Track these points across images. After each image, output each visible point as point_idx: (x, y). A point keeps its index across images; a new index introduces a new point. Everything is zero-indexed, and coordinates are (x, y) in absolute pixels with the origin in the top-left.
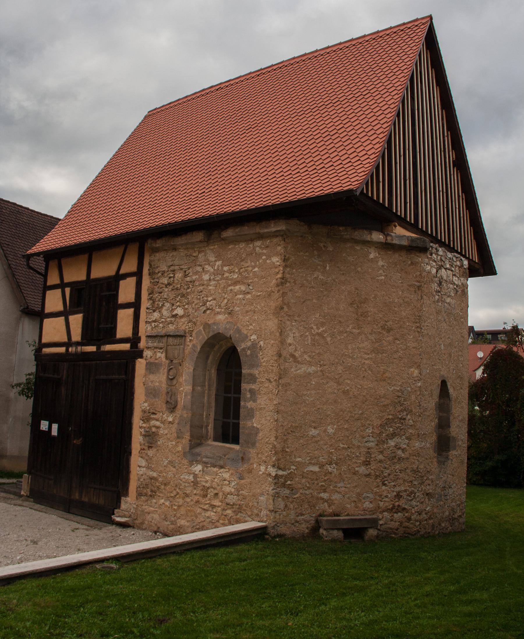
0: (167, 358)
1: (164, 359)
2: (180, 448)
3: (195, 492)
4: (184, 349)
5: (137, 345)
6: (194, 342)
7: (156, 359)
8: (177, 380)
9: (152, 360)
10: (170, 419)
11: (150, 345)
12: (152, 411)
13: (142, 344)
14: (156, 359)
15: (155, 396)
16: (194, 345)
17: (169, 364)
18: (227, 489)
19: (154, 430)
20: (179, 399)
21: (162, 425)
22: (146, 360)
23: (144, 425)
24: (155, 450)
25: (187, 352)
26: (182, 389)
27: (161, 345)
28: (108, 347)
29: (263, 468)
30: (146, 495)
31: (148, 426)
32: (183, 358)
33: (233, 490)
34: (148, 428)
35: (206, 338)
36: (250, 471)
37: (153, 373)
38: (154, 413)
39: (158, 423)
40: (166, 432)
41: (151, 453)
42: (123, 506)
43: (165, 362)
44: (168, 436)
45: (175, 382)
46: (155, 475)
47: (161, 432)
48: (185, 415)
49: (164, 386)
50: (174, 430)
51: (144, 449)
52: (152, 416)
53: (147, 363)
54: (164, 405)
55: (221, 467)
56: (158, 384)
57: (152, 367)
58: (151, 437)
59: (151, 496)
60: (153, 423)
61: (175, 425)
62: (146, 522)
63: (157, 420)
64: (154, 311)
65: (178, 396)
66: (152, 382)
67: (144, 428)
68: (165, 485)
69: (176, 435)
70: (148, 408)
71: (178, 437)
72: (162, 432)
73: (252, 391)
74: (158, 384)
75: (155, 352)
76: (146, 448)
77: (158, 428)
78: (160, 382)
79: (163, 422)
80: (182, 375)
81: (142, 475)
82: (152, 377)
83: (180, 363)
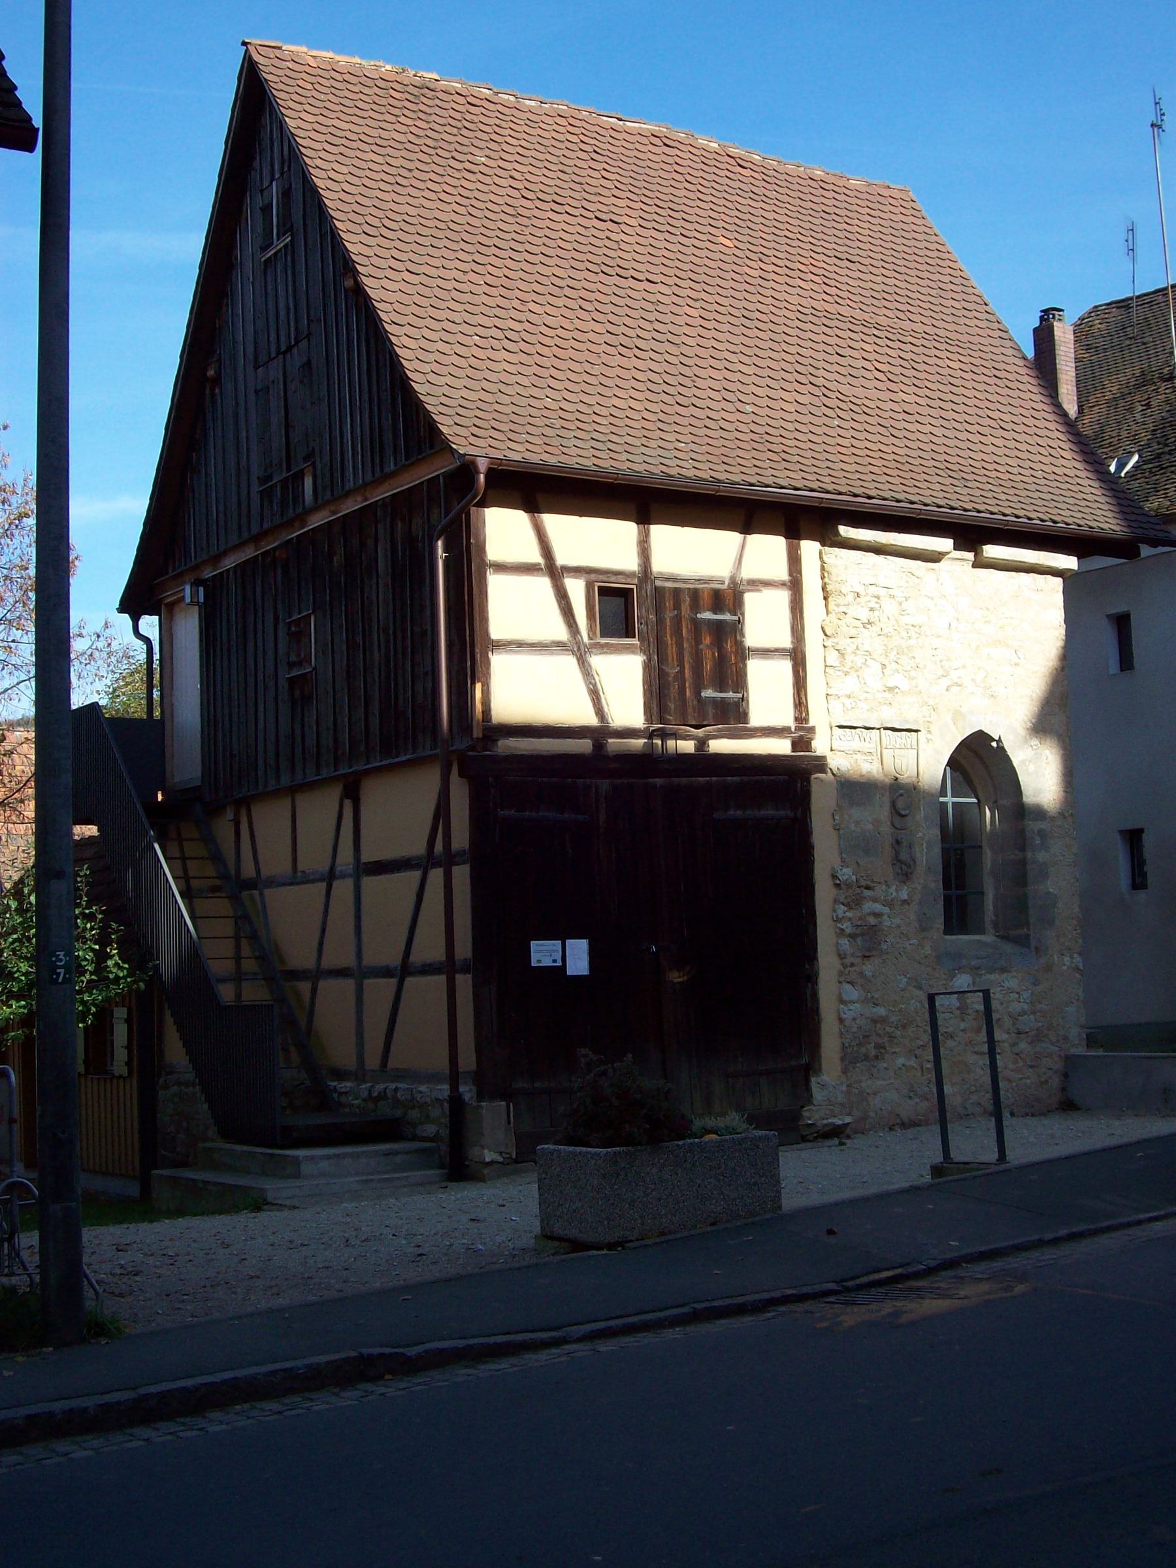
2: (928, 950)
3: (962, 1025)
10: (904, 895)
12: (863, 883)
18: (1016, 1007)
19: (872, 921)
20: (918, 855)
21: (886, 910)
24: (877, 961)
28: (721, 746)
29: (1067, 959)
30: (866, 1058)
31: (859, 914)
33: (1026, 1007)
34: (860, 918)
36: (1048, 968)
38: (868, 888)
39: (878, 907)
40: (897, 921)
41: (868, 968)
42: (818, 1095)
46: (881, 1011)
48: (933, 885)
49: (886, 829)
50: (913, 917)
51: (852, 965)
52: (867, 893)
55: (1003, 970)
56: (870, 827)
58: (868, 938)
59: (876, 1057)
60: (868, 906)
62: (872, 1114)
63: (875, 900)
64: (846, 674)
66: (857, 823)
67: (850, 919)
68: (904, 1027)
72: (888, 924)
73: (1041, 833)
74: (870, 827)
76: (857, 961)
77: (877, 915)
79: (889, 904)
81: (854, 1019)
82: (856, 813)
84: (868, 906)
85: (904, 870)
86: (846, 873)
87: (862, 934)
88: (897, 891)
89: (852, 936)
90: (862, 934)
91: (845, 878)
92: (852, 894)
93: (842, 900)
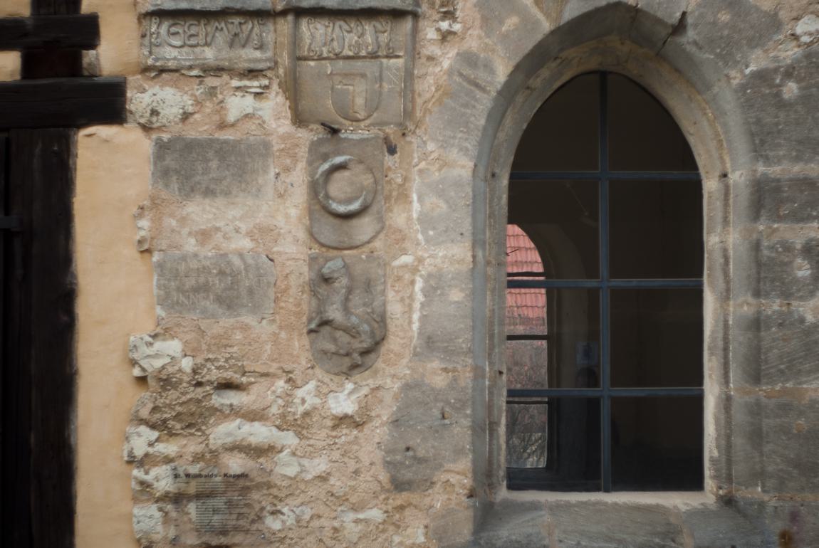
0: (299, 119)
1: (284, 126)
4: (409, 76)
5: (77, 59)
6: (473, 42)
7: (223, 126)
8: (381, 220)
9: (199, 130)
10: (344, 402)
11: (171, 54)
12: (215, 375)
13: (110, 55)
14: (223, 126)
15: (229, 302)
16: (468, 59)
17: (314, 146)
19: (235, 464)
20: (395, 309)
21: (289, 439)
22: (146, 128)
23: (169, 448)
25: (427, 87)
26: (406, 259)
27: (248, 56)
32: (409, 114)
34: (198, 458)
35: (546, 26)
37: (209, 193)
38: (228, 386)
39: (259, 433)
40: (319, 465)
43: (284, 138)
44: (336, 483)
45: (364, 228)
47: (286, 467)
53: (162, 149)
54: (300, 346)
56: (246, 244)
57: (191, 164)
61: (378, 431)
63: (254, 416)
65: (391, 295)
66: (204, 236)
67: (168, 460)
69: (384, 477)
70: (187, 364)
71: (399, 485)
72: (291, 471)
74: (246, 244)
75: (212, 92)
78: (264, 233)
79: (299, 424)
80: (404, 197)
82: (200, 212)
83: (386, 140)
84: (223, 432)
85: (350, 343)
86: (169, 352)
87: (198, 496)
88: (318, 393)
89: (178, 499)
90: (198, 496)
91: (158, 363)
92: (176, 405)
93: (145, 413)
